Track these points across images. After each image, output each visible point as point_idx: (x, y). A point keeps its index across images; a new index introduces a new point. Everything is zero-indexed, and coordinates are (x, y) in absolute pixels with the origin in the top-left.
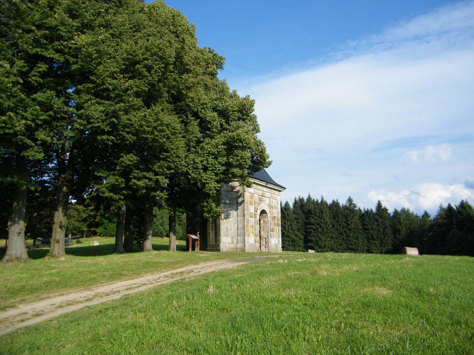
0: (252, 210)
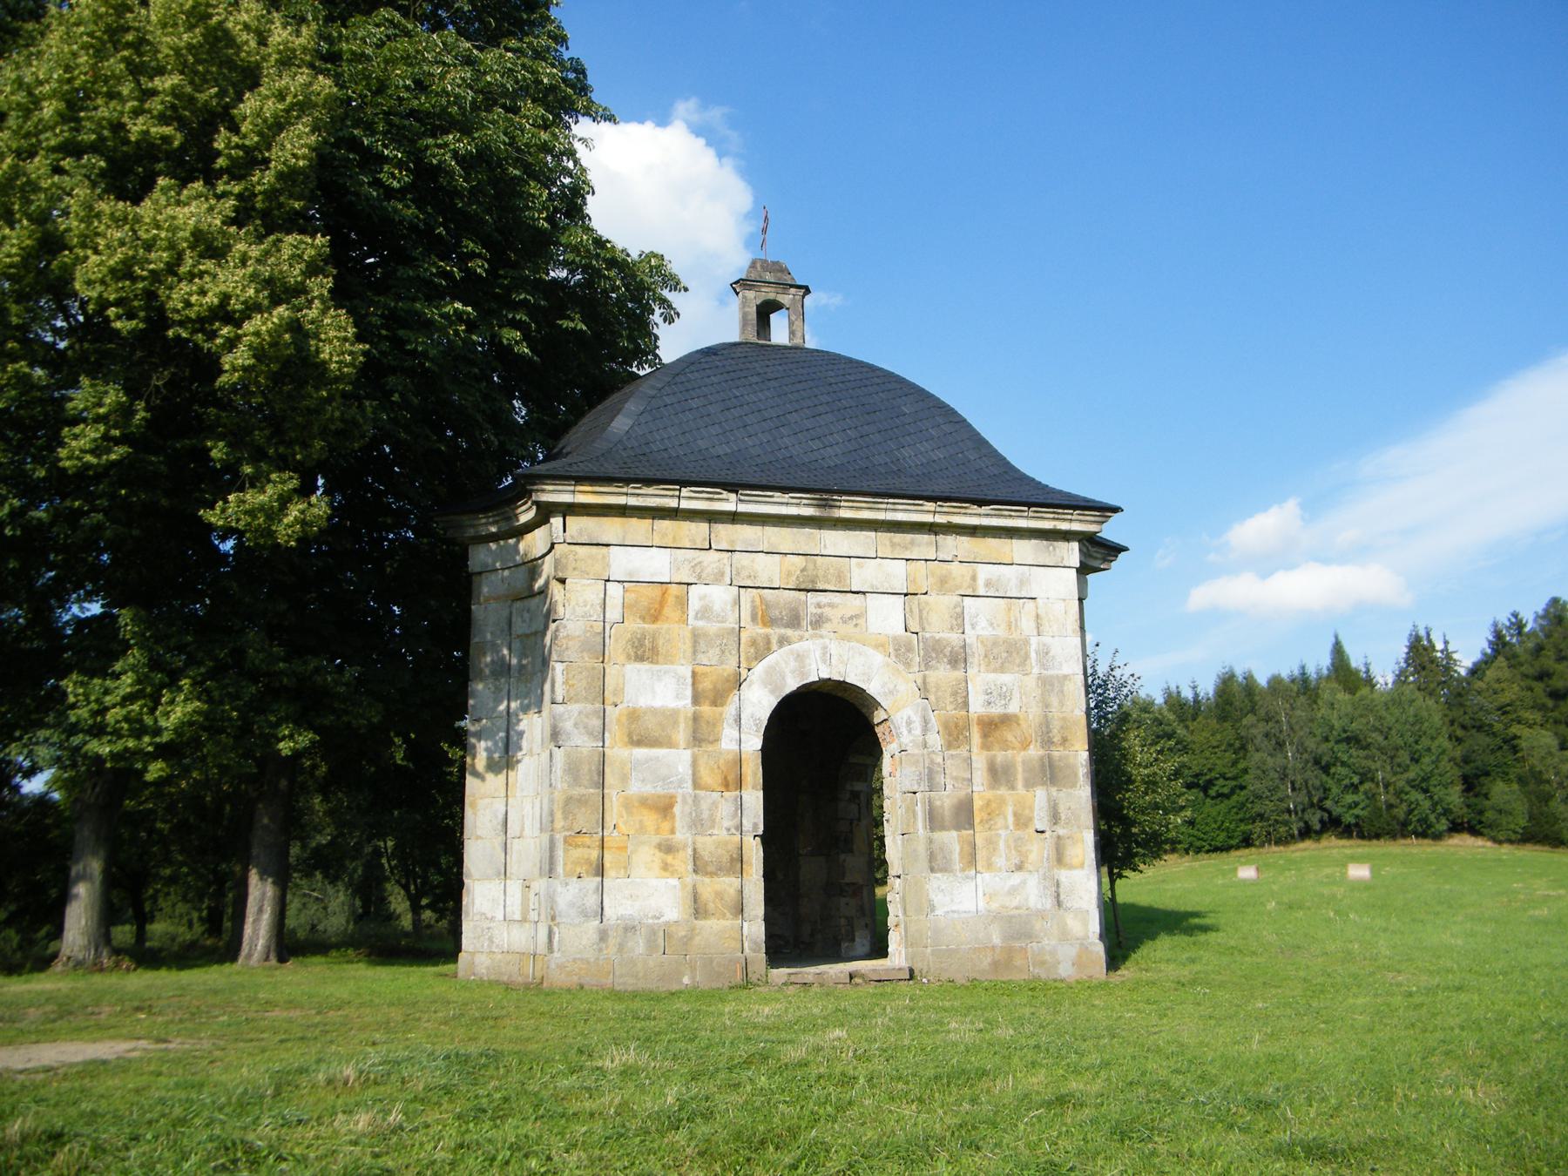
0: (660, 690)
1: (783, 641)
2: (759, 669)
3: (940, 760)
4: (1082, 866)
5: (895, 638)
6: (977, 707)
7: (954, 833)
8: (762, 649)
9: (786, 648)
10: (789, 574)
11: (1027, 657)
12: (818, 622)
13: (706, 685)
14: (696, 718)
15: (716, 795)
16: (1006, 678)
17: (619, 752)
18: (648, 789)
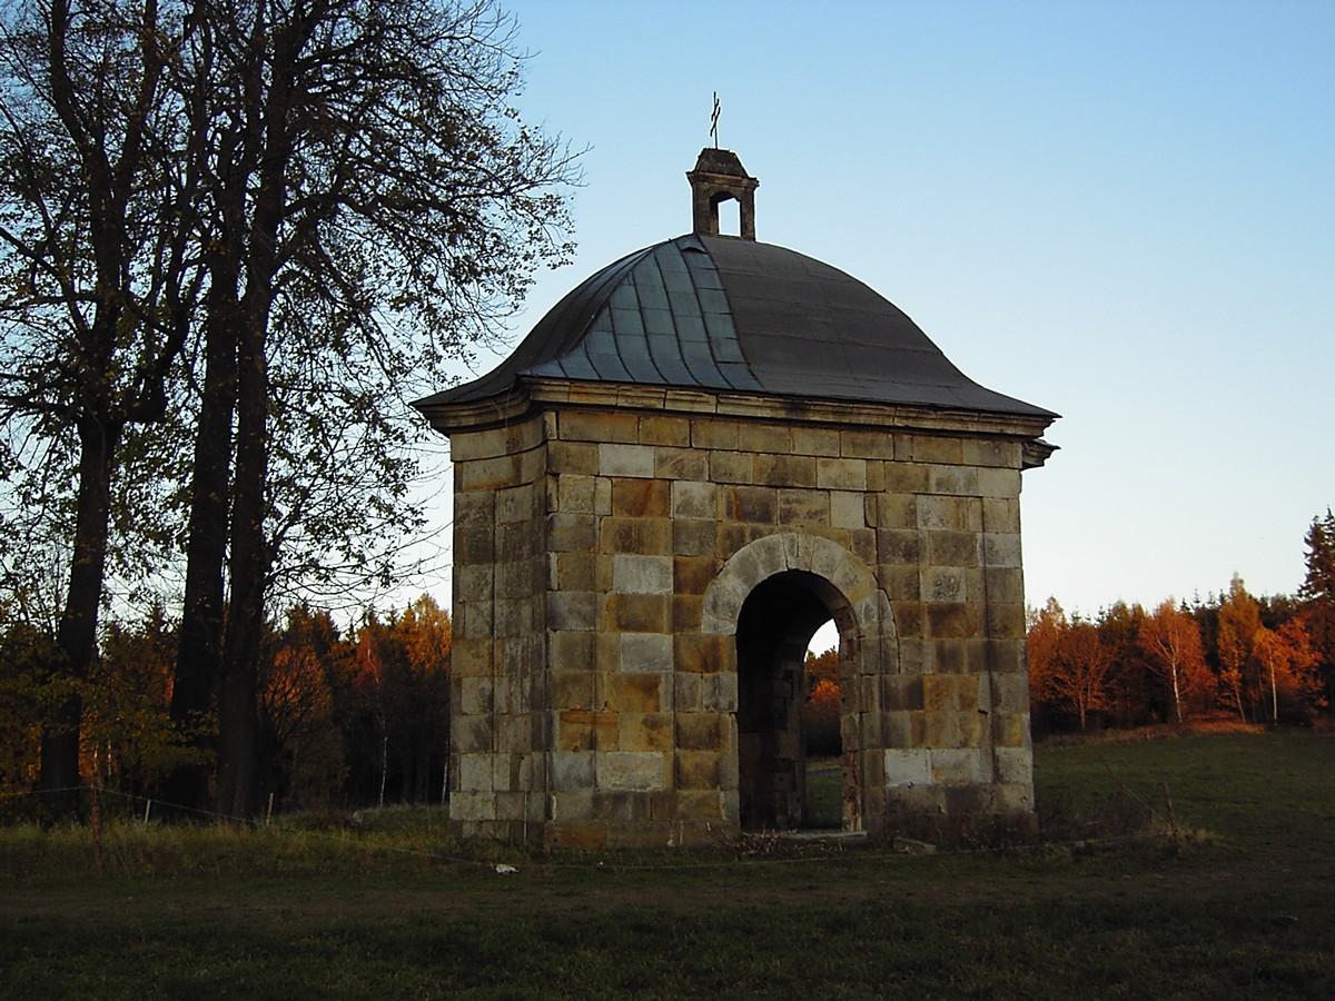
1: (756, 534)
2: (735, 558)
3: (895, 645)
5: (856, 532)
6: (927, 596)
8: (735, 542)
10: (761, 471)
11: (973, 551)
12: (787, 517)
13: (687, 573)
14: (677, 606)
16: (954, 570)
17: (608, 635)
18: (636, 670)
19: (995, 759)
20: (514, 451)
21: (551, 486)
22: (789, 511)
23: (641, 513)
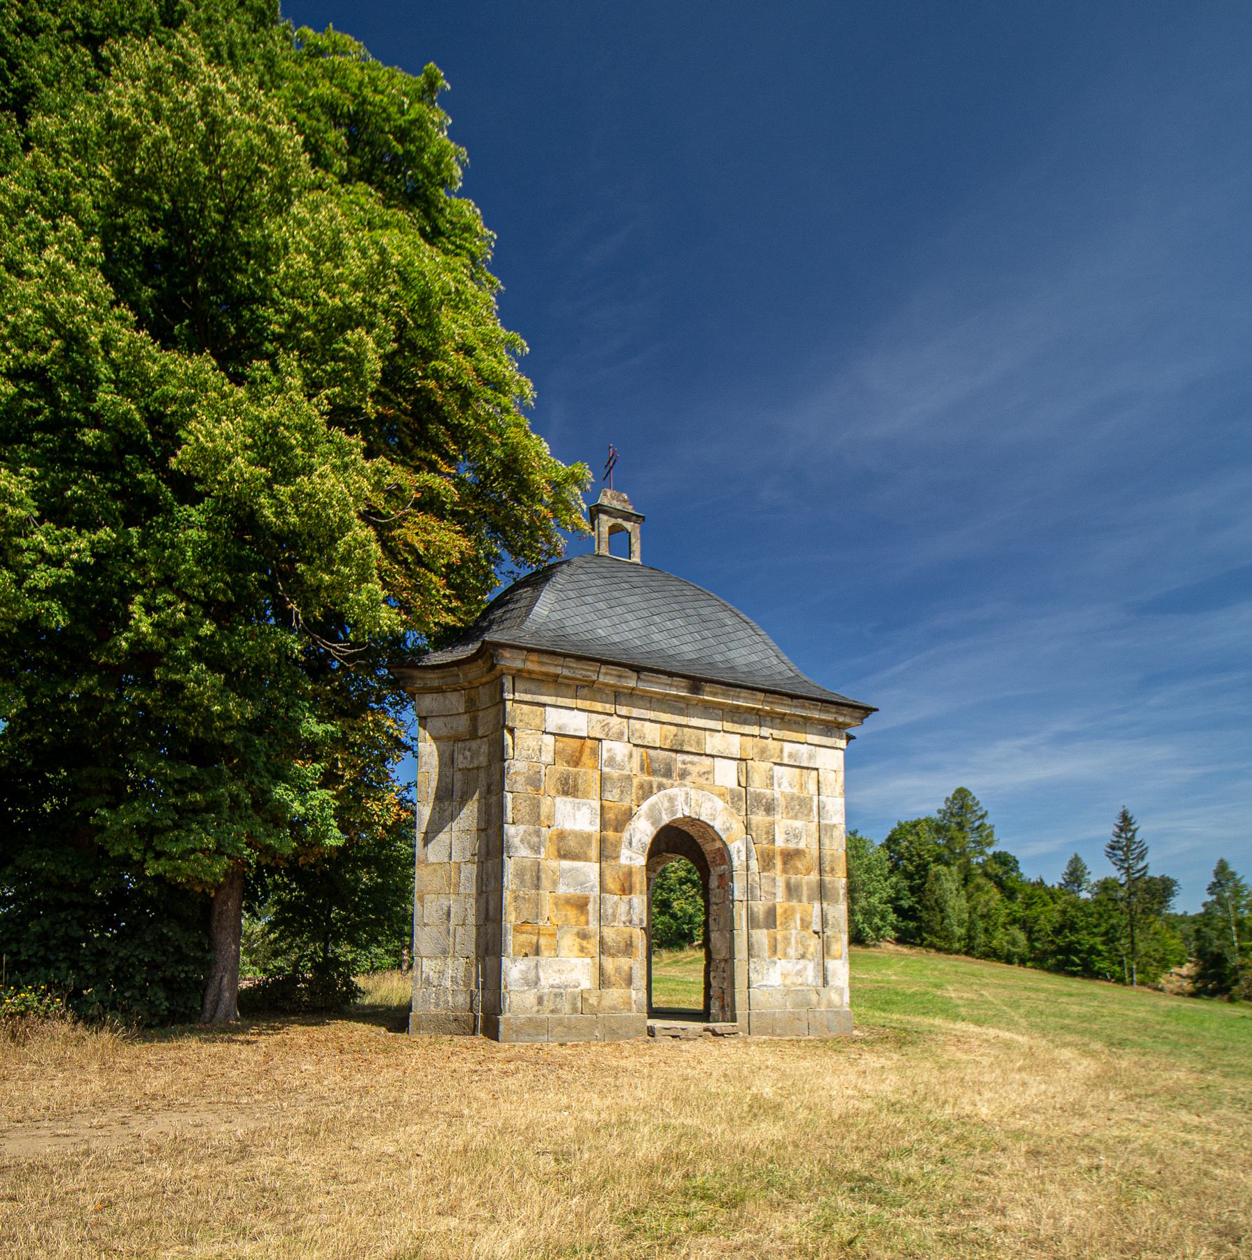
0: (577, 817)
1: (661, 787)
2: (646, 805)
3: (757, 879)
4: (840, 957)
5: (731, 790)
6: (780, 843)
7: (765, 931)
9: (662, 792)
10: (666, 738)
11: (811, 810)
12: (683, 775)
13: (610, 816)
14: (602, 841)
15: (616, 898)
16: (798, 824)
18: (571, 890)
19: (825, 969)
20: (472, 707)
21: (508, 737)
22: (685, 770)
23: (576, 764)
